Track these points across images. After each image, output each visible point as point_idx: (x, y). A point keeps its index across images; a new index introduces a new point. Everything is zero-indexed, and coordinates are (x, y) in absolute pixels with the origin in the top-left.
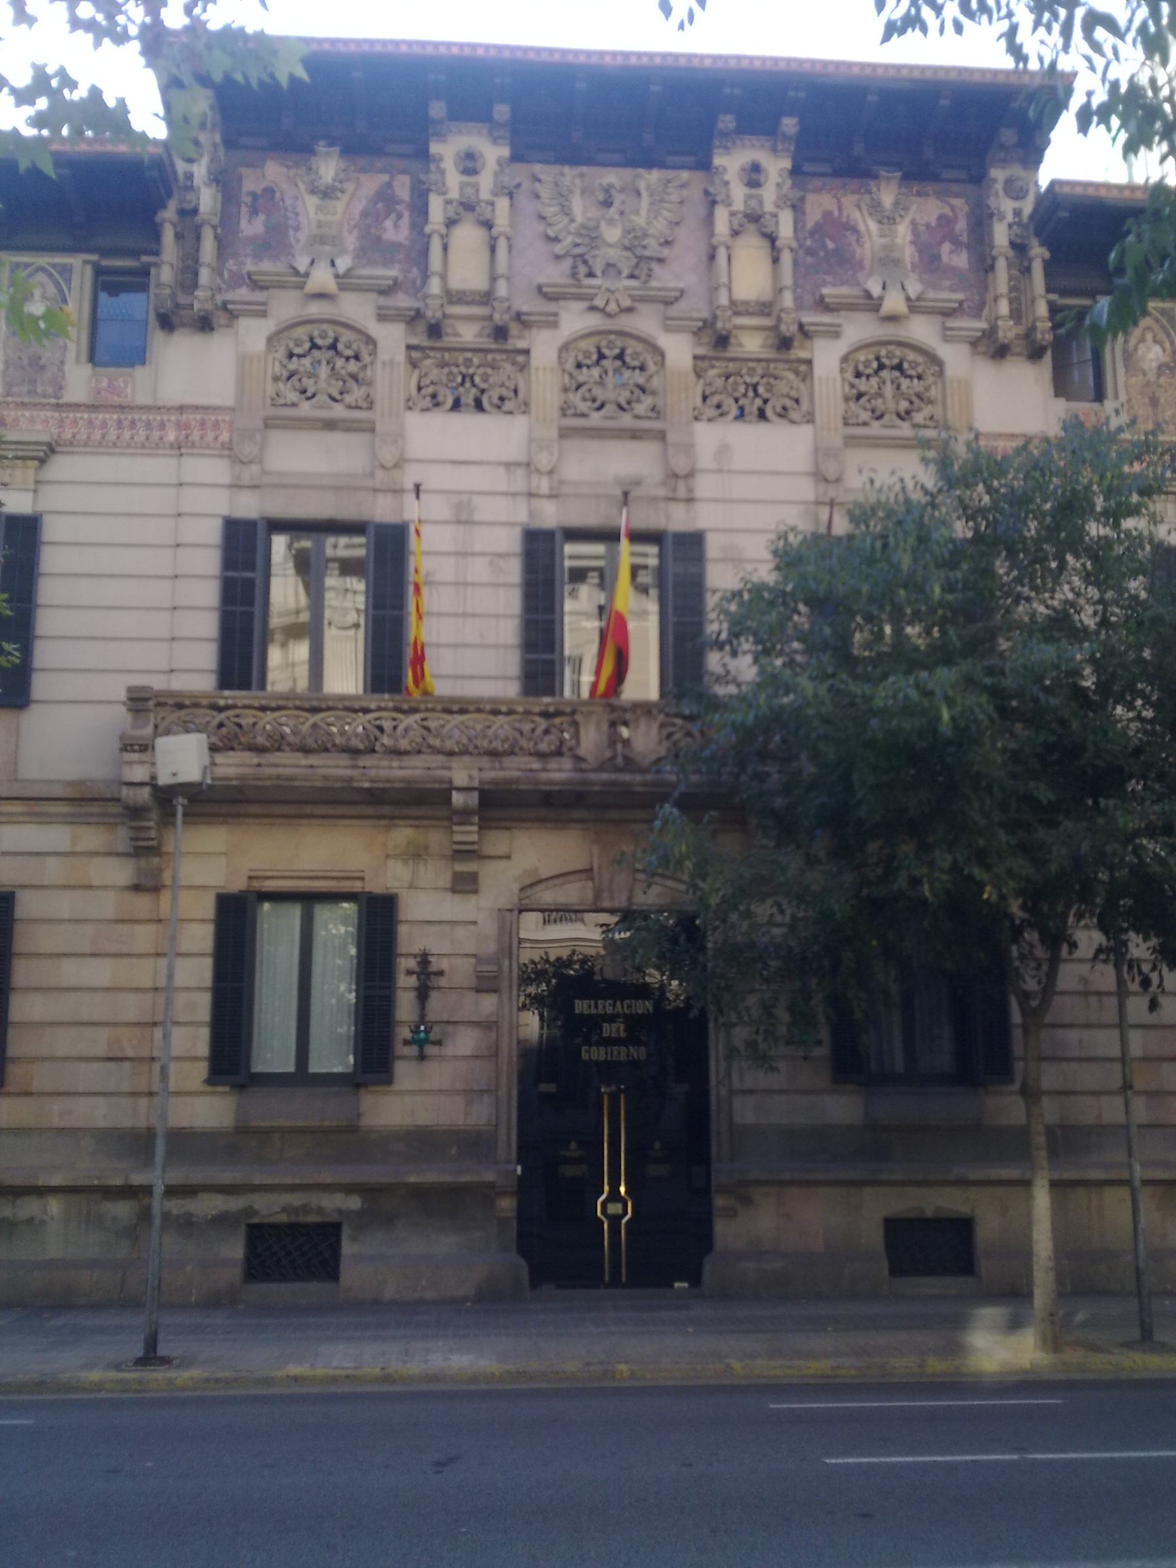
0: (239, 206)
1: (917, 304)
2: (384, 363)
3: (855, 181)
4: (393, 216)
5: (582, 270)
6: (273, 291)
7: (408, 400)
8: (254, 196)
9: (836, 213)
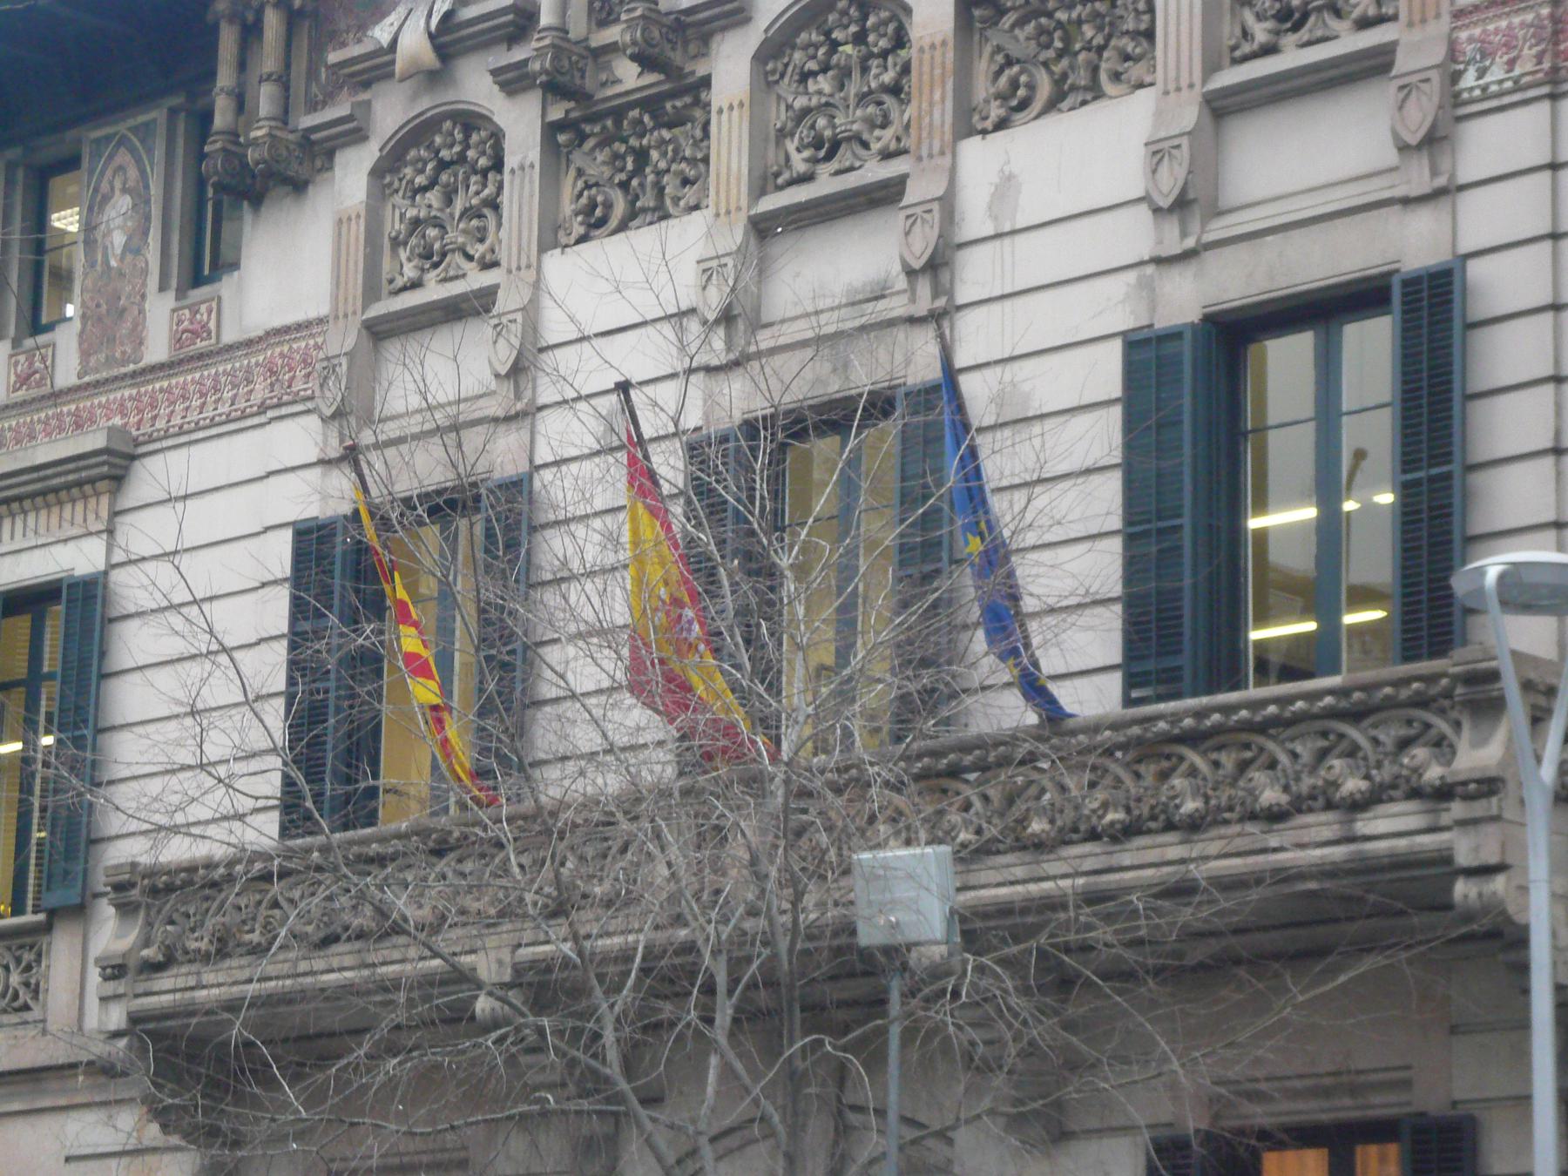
1: (447, 38)
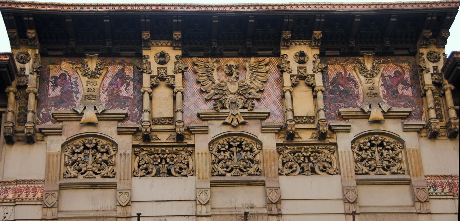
0: (48, 83)
2: (121, 154)
3: (352, 58)
4: (125, 85)
5: (219, 105)
6: (64, 123)
7: (134, 172)
8: (54, 77)
9: (343, 73)
